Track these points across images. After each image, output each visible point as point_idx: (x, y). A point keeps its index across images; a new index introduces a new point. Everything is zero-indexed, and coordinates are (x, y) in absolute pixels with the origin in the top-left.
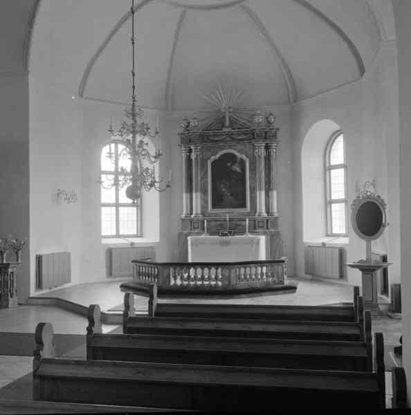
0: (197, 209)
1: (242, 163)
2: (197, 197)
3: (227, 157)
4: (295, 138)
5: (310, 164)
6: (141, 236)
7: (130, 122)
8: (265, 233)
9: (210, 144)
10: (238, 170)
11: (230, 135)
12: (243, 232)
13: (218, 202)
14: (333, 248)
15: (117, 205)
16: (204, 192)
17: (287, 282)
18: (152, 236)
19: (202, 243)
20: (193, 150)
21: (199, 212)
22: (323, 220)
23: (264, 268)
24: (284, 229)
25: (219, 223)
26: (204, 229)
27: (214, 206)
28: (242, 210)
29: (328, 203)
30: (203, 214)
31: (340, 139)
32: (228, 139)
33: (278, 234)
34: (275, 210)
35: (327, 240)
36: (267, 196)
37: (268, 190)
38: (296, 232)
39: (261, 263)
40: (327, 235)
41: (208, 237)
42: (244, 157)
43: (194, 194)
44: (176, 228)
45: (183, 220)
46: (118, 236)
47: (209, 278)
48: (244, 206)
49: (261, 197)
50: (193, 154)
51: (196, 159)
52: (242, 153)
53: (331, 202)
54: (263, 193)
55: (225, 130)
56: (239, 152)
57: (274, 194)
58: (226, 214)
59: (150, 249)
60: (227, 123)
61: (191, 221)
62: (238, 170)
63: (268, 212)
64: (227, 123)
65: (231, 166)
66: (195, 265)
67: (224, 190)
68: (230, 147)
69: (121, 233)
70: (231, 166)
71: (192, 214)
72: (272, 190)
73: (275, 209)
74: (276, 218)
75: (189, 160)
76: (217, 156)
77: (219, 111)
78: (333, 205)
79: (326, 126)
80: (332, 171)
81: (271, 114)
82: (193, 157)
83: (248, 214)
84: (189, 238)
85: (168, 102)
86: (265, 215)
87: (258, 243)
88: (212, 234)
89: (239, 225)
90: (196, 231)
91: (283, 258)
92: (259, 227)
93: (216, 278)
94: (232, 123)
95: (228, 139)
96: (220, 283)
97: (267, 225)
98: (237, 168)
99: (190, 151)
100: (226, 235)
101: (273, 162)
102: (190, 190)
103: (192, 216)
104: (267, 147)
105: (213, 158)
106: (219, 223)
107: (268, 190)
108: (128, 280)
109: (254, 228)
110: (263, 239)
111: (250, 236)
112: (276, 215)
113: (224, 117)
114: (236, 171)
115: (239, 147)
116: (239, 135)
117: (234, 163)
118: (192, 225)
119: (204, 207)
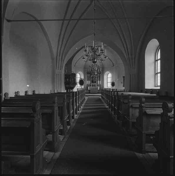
0: (89, 83)
3: (94, 75)
5: (105, 77)
14: (109, 89)
29: (107, 83)
35: (108, 88)
36: (99, 81)
37: (99, 80)
38: (103, 87)
48: (96, 83)
57: (100, 81)
58: (94, 84)
63: (99, 83)
73: (100, 83)
102: (88, 81)
107: (99, 80)
119: (90, 83)
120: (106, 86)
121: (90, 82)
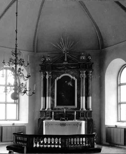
0: (49, 105)
1: (73, 81)
2: (49, 99)
4: (102, 68)
6: (18, 120)
7: (14, 58)
8: (84, 120)
10: (71, 85)
11: (67, 66)
12: (72, 119)
15: (6, 103)
16: (53, 96)
17: (96, 146)
18: (24, 120)
19: (52, 124)
20: (47, 74)
21: (50, 107)
22: (116, 112)
23: (84, 139)
24: (95, 119)
25: (60, 113)
26: (51, 116)
27: (58, 104)
28: (72, 107)
30: (52, 108)
31: (125, 68)
33: (91, 120)
34: (90, 107)
36: (86, 100)
39: (82, 136)
40: (118, 121)
41: (54, 121)
42: (74, 78)
43: (47, 98)
44: (37, 116)
45: (41, 112)
46: (6, 120)
47: (54, 144)
48: (74, 104)
49: (83, 99)
50: (47, 76)
51: (49, 79)
52: (73, 76)
53: (120, 104)
54: (84, 98)
55: (64, 63)
56: (72, 75)
57: (90, 98)
58: (64, 109)
59: (23, 128)
60: (66, 60)
61: (45, 112)
62: (71, 85)
64: (66, 60)
65: (67, 83)
66: (47, 136)
68: (67, 73)
69: (8, 118)
71: (46, 108)
73: (90, 106)
74: (91, 112)
75: (45, 80)
76: (60, 77)
77: (61, 53)
78: (121, 105)
79: (120, 62)
80: (121, 86)
81: (89, 55)
82: (47, 77)
83: (76, 109)
84: (44, 121)
85: (35, 48)
86: (85, 109)
87: (81, 125)
88: (56, 119)
91: (94, 133)
93: (58, 144)
94: (68, 60)
96: (60, 146)
97: (86, 115)
98: (70, 84)
99: (46, 74)
100: (64, 120)
101: (90, 81)
102: (45, 96)
103: (46, 110)
104: (87, 73)
105: (58, 78)
108: (10, 144)
109: (78, 118)
110: (83, 123)
111: (76, 121)
112: (91, 109)
113: (64, 57)
116: (72, 66)
118: (45, 114)
119: (52, 105)
120: (115, 119)
121: (53, 101)
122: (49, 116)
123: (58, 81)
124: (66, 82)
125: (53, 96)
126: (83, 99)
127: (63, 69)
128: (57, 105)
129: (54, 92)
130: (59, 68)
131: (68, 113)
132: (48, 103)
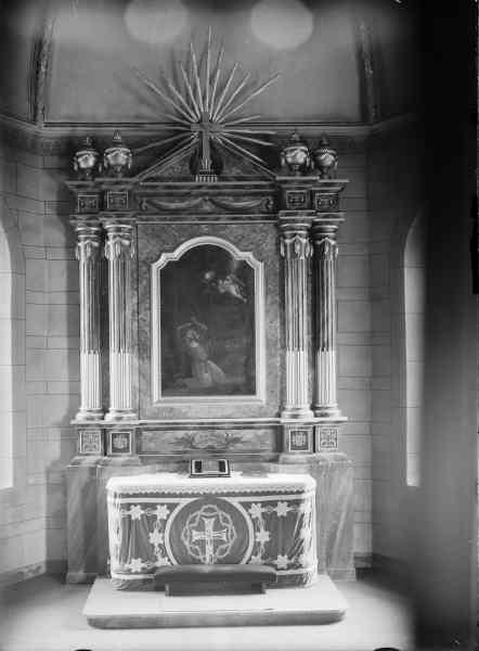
1: (245, 273)
2: (122, 362)
9: (157, 221)
10: (234, 290)
11: (213, 196)
13: (178, 375)
16: (143, 349)
20: (110, 234)
21: (128, 405)
25: (180, 434)
27: (168, 386)
32: (207, 207)
36: (314, 364)
43: (113, 356)
48: (252, 391)
50: (110, 243)
51: (122, 256)
54: (304, 355)
55: (199, 180)
62: (234, 290)
63: (314, 408)
64: (206, 163)
65: (215, 280)
67: (195, 345)
68: (214, 232)
70: (215, 280)
71: (105, 410)
72: (326, 346)
76: (177, 254)
82: (112, 252)
86: (308, 416)
89: (237, 440)
90: (123, 458)
92: (295, 447)
94: (217, 168)
95: (207, 207)
99: (102, 236)
102: (103, 346)
103: (110, 418)
104: (315, 234)
105: (163, 260)
106: (180, 434)
114: (227, 295)
115: (235, 228)
116: (237, 197)
117: (222, 273)
119: (142, 391)
122: (126, 450)
123: (165, 274)
124: (208, 276)
125: (143, 349)
126: (298, 360)
127: (194, 211)
128: (163, 394)
129: (147, 329)
130: (173, 206)
131: (222, 432)
132: (126, 380)
